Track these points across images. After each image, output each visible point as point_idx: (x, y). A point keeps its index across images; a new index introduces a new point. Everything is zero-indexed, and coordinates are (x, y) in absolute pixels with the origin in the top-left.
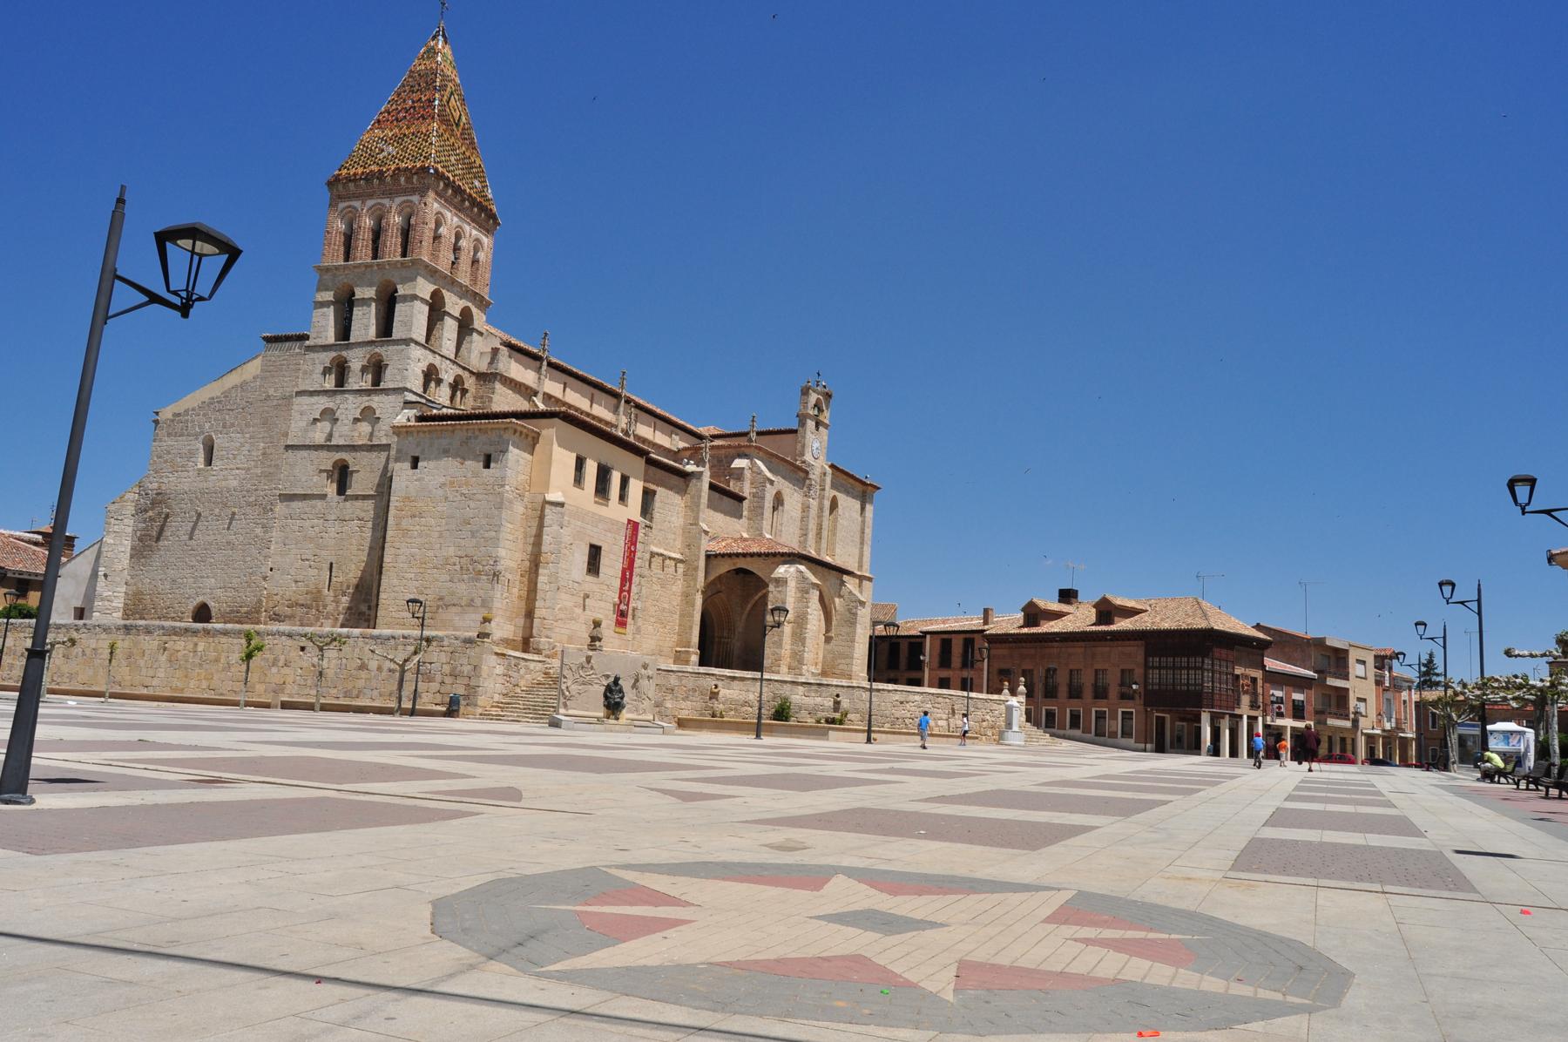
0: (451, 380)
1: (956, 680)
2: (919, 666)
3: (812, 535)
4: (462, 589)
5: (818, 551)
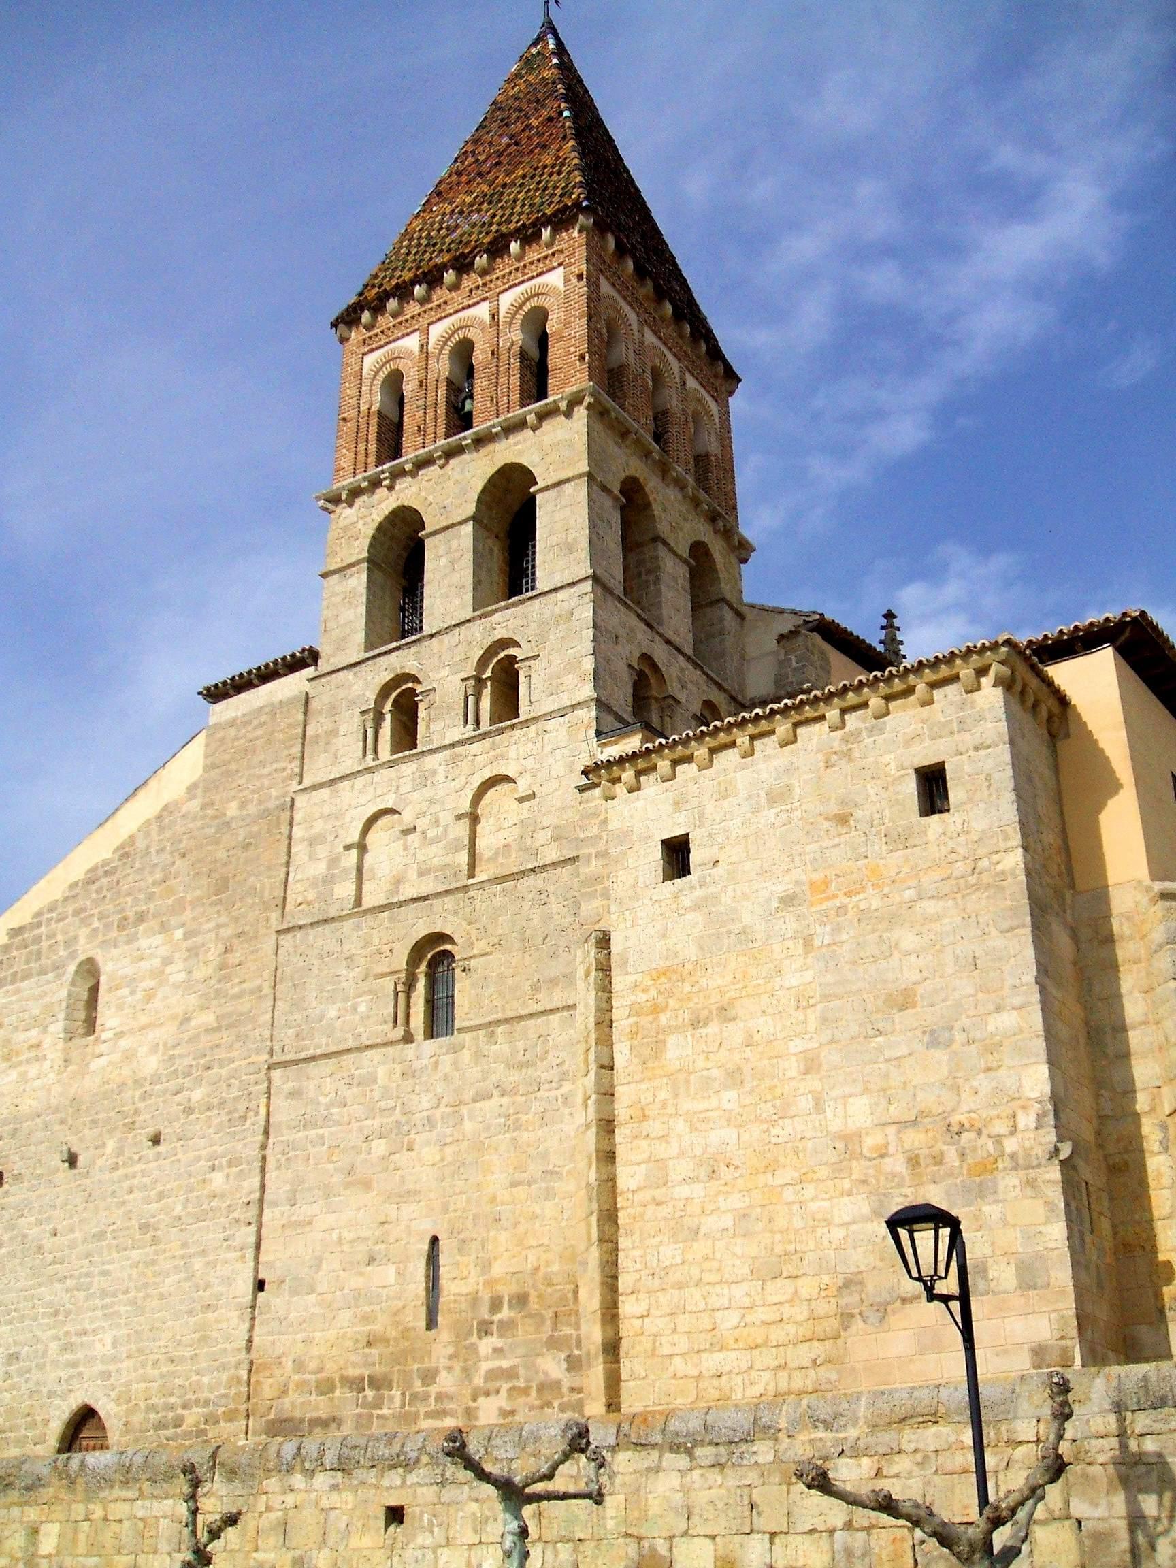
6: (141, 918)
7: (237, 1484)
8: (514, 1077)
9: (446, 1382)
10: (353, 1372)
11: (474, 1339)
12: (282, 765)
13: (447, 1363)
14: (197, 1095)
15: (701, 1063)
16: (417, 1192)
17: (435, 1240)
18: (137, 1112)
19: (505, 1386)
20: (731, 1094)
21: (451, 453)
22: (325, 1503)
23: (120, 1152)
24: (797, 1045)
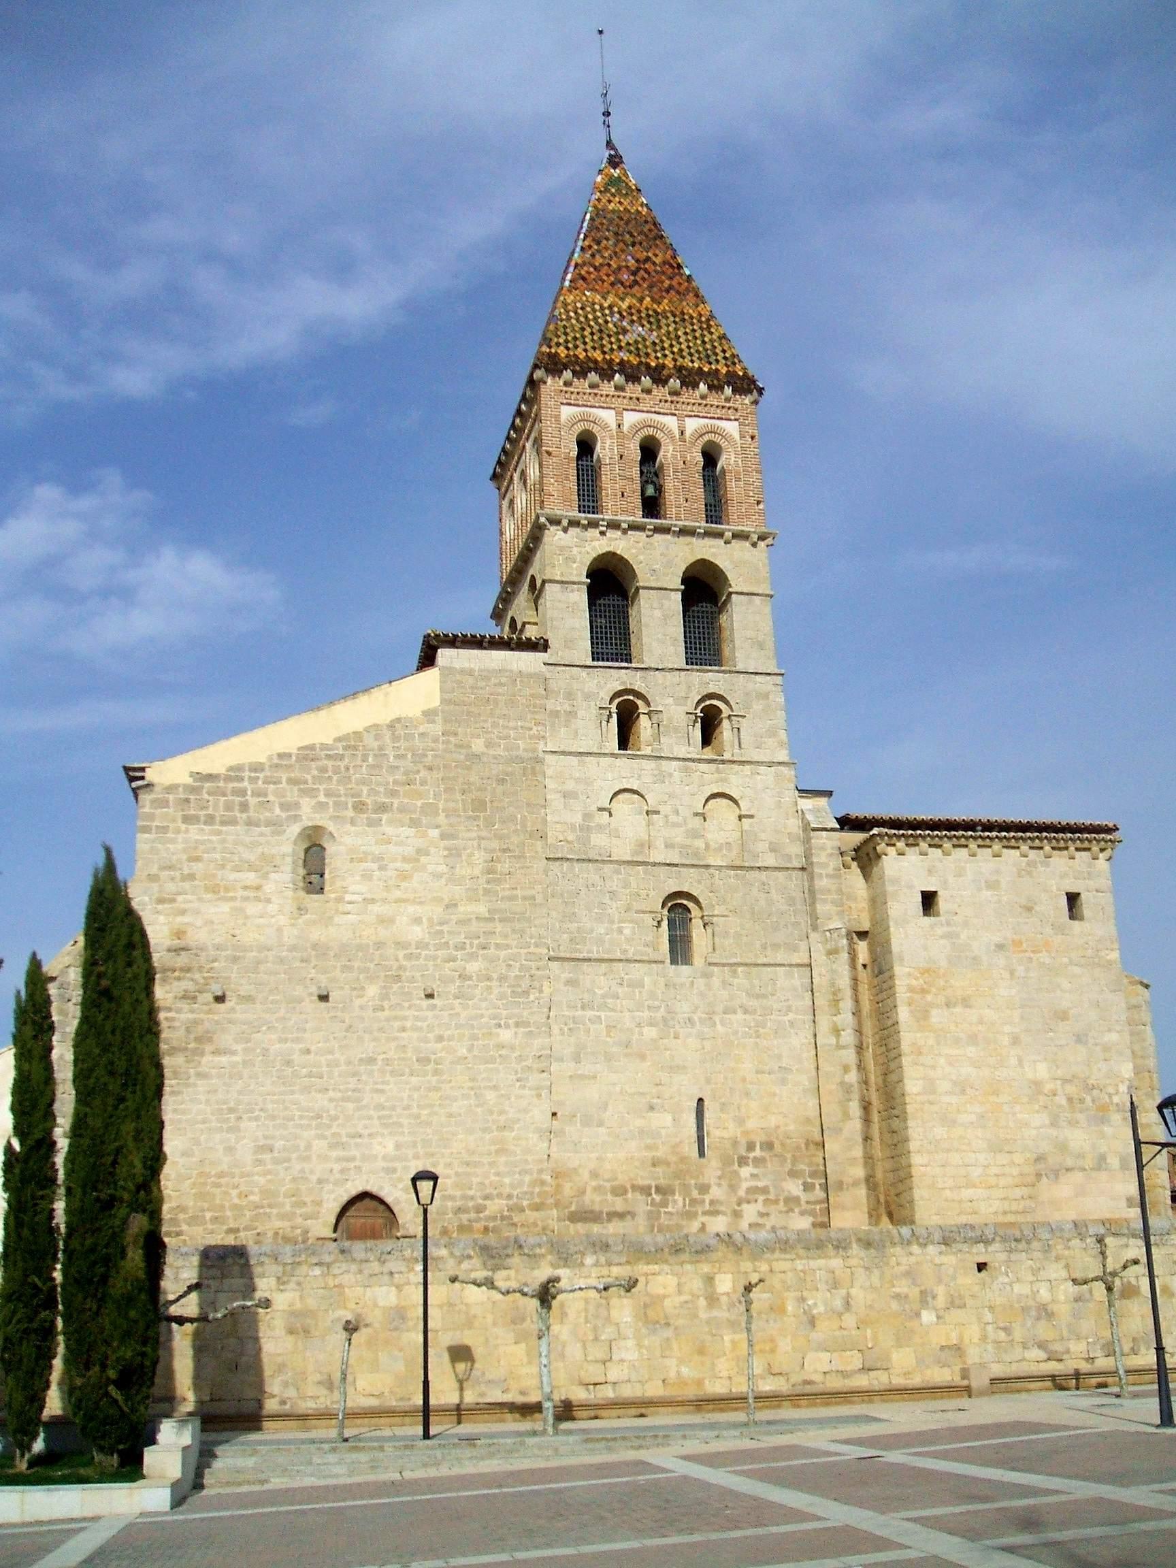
4: (1078, 1138)
6: (383, 808)
7: (872, 1251)
8: (753, 1003)
9: (716, 1192)
10: (641, 1182)
11: (736, 1167)
12: (527, 725)
13: (717, 1181)
14: (473, 967)
15: (953, 1028)
16: (684, 1067)
17: (700, 1100)
18: (400, 968)
19: (761, 1198)
20: (972, 1049)
22: (937, 1261)
23: (385, 997)
24: (1007, 1029)
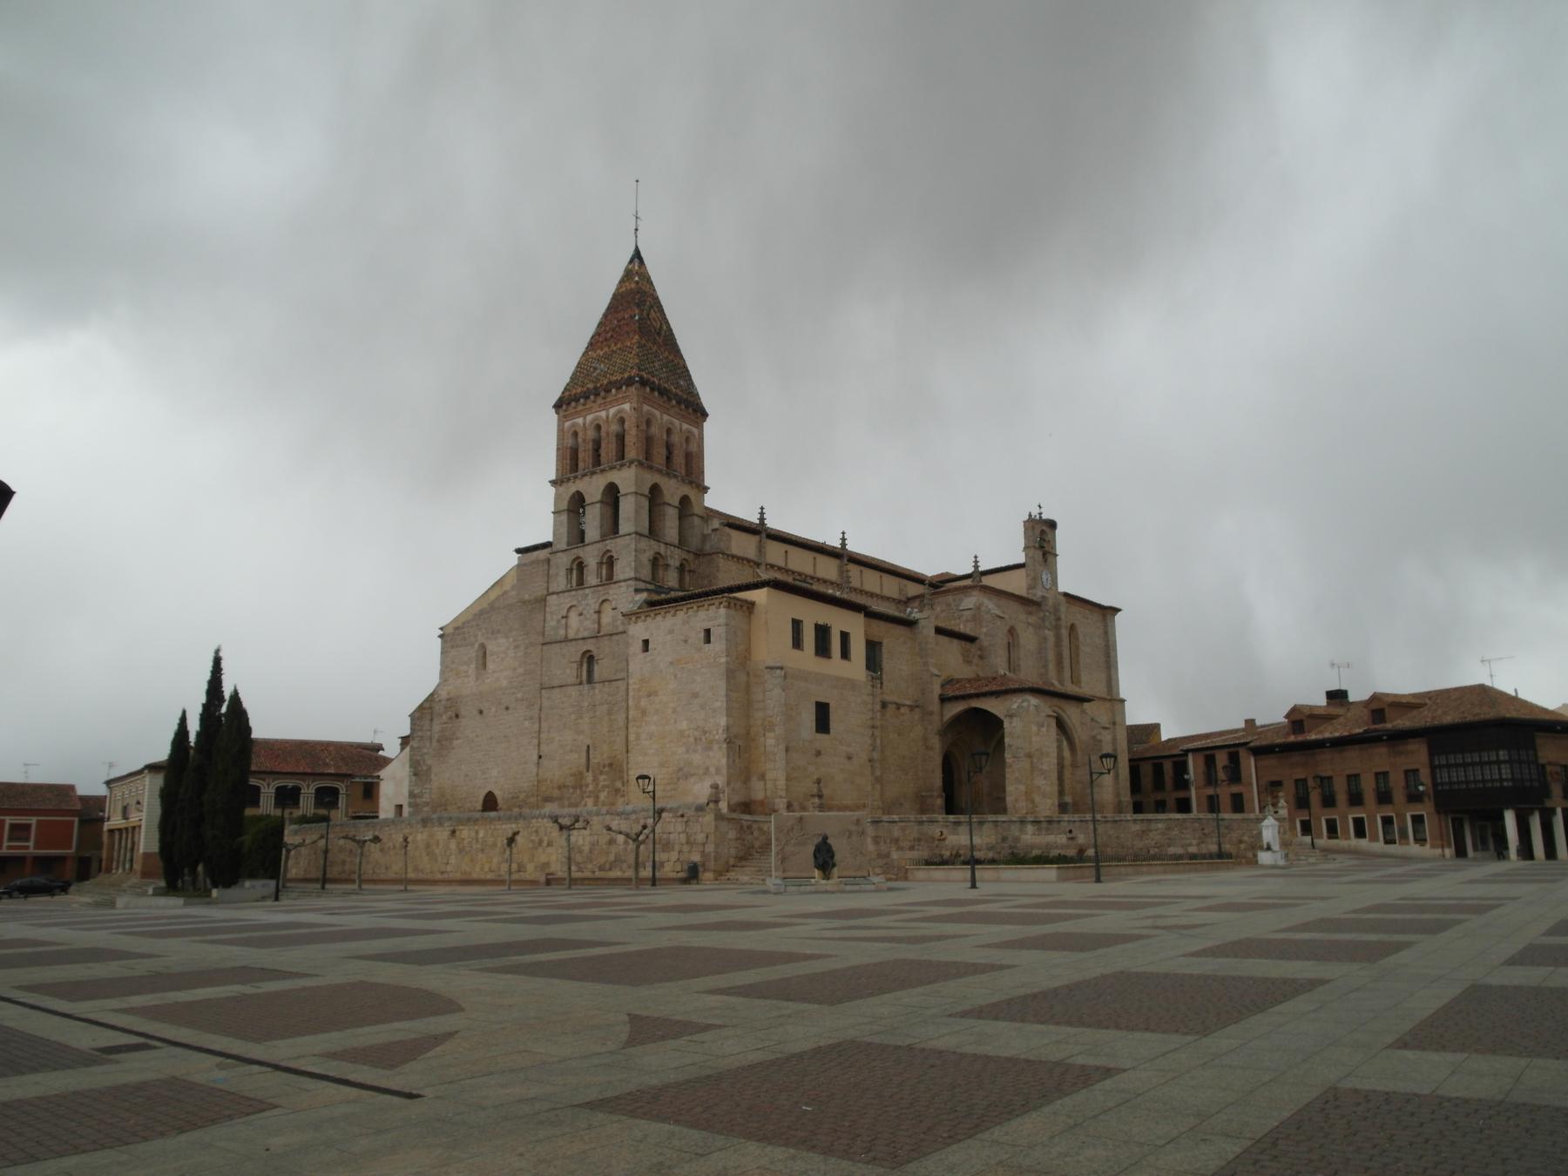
0: (677, 564)
1: (1171, 802)
2: (1182, 784)
3: (1052, 667)
4: (697, 758)
5: (1061, 682)
9: (591, 788)
21: (593, 473)
